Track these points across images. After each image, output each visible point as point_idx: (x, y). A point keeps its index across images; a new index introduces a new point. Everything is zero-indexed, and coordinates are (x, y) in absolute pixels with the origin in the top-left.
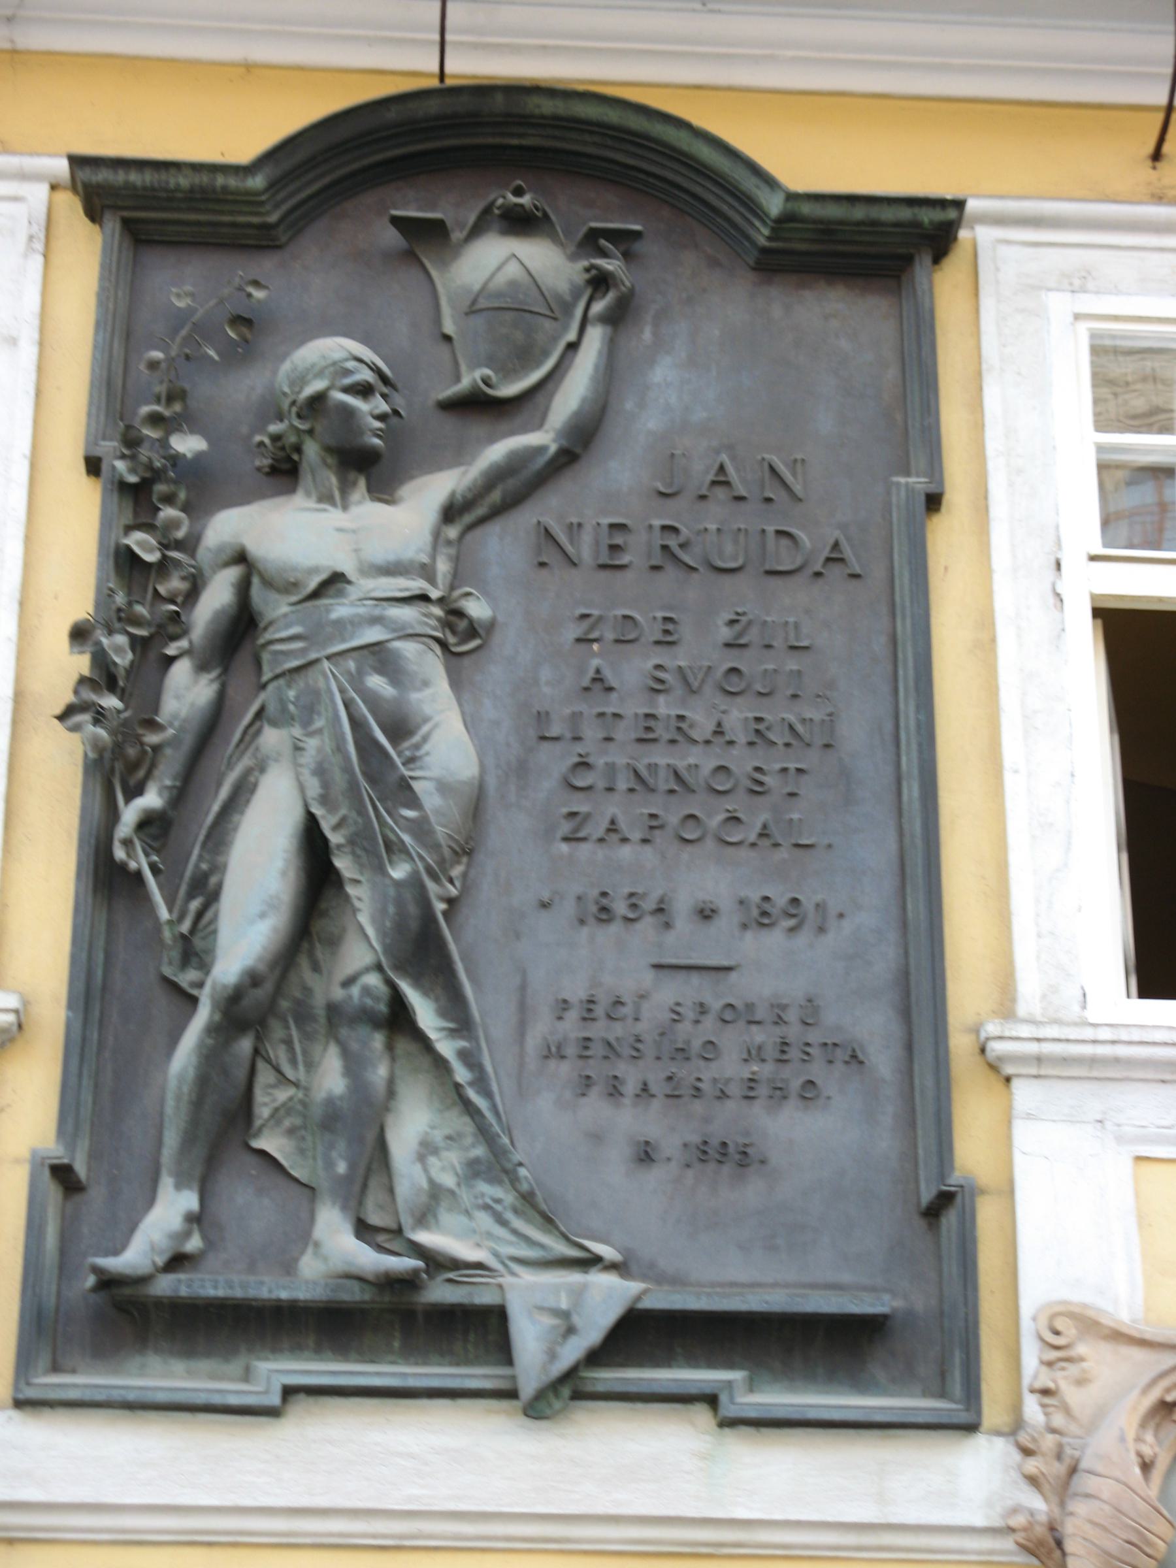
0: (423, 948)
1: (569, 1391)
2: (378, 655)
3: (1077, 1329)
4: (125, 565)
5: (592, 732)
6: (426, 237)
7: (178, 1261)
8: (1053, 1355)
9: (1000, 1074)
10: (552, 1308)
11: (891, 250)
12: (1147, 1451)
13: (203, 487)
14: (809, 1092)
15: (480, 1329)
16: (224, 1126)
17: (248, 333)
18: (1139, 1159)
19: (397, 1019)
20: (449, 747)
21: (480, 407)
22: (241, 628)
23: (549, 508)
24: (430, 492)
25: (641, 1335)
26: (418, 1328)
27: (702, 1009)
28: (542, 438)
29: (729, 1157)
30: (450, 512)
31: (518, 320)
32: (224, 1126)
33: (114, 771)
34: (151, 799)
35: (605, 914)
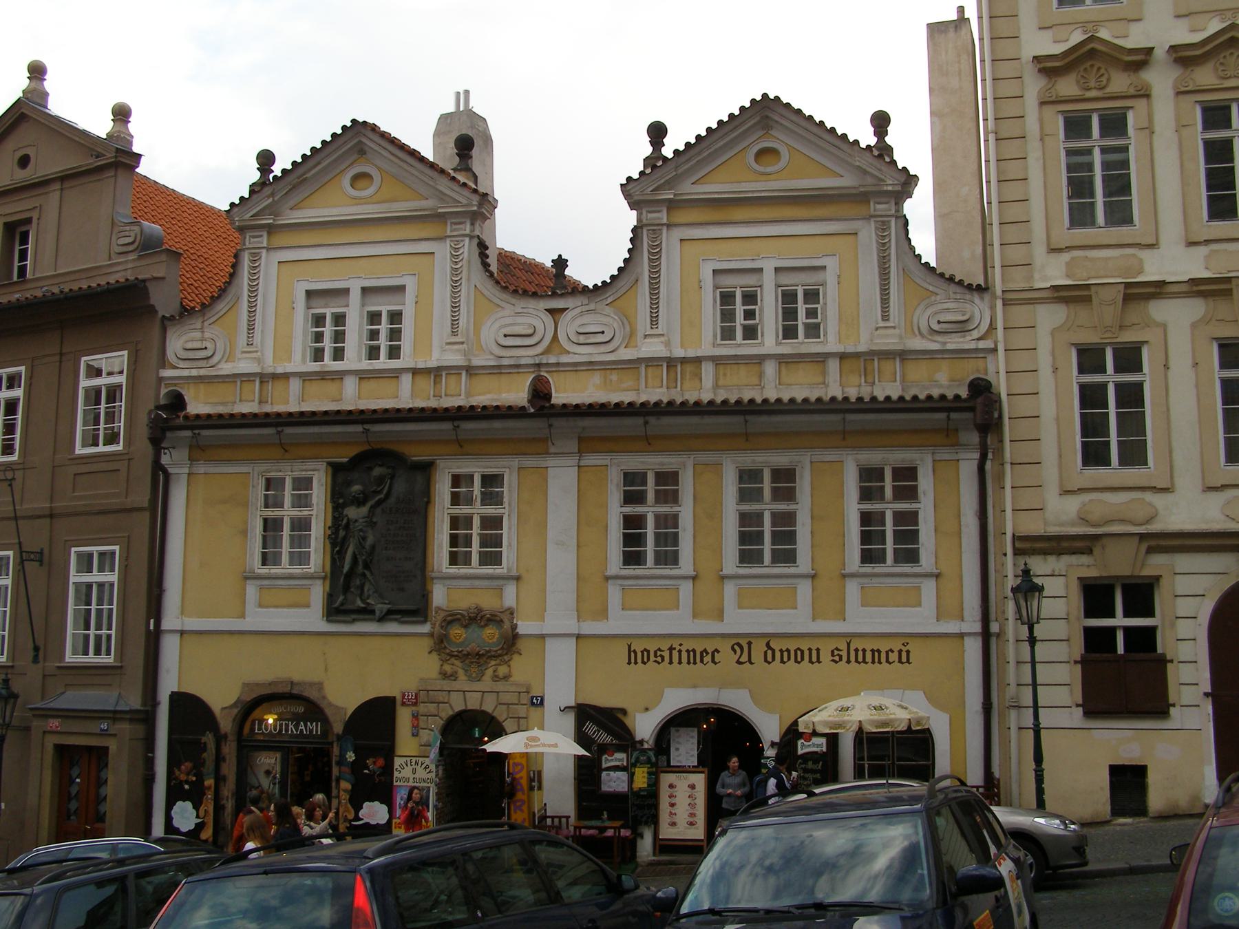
0: (367, 566)
1: (381, 620)
2: (361, 530)
3: (439, 609)
4: (334, 518)
6: (370, 469)
7: (342, 604)
9: (433, 579)
10: (381, 608)
11: (426, 468)
13: (344, 505)
15: (373, 612)
16: (346, 589)
17: (349, 484)
19: (364, 575)
20: (370, 540)
21: (376, 492)
22: (347, 527)
25: (390, 612)
26: (366, 613)
29: (402, 590)
31: (380, 480)
32: (346, 589)
33: (333, 545)
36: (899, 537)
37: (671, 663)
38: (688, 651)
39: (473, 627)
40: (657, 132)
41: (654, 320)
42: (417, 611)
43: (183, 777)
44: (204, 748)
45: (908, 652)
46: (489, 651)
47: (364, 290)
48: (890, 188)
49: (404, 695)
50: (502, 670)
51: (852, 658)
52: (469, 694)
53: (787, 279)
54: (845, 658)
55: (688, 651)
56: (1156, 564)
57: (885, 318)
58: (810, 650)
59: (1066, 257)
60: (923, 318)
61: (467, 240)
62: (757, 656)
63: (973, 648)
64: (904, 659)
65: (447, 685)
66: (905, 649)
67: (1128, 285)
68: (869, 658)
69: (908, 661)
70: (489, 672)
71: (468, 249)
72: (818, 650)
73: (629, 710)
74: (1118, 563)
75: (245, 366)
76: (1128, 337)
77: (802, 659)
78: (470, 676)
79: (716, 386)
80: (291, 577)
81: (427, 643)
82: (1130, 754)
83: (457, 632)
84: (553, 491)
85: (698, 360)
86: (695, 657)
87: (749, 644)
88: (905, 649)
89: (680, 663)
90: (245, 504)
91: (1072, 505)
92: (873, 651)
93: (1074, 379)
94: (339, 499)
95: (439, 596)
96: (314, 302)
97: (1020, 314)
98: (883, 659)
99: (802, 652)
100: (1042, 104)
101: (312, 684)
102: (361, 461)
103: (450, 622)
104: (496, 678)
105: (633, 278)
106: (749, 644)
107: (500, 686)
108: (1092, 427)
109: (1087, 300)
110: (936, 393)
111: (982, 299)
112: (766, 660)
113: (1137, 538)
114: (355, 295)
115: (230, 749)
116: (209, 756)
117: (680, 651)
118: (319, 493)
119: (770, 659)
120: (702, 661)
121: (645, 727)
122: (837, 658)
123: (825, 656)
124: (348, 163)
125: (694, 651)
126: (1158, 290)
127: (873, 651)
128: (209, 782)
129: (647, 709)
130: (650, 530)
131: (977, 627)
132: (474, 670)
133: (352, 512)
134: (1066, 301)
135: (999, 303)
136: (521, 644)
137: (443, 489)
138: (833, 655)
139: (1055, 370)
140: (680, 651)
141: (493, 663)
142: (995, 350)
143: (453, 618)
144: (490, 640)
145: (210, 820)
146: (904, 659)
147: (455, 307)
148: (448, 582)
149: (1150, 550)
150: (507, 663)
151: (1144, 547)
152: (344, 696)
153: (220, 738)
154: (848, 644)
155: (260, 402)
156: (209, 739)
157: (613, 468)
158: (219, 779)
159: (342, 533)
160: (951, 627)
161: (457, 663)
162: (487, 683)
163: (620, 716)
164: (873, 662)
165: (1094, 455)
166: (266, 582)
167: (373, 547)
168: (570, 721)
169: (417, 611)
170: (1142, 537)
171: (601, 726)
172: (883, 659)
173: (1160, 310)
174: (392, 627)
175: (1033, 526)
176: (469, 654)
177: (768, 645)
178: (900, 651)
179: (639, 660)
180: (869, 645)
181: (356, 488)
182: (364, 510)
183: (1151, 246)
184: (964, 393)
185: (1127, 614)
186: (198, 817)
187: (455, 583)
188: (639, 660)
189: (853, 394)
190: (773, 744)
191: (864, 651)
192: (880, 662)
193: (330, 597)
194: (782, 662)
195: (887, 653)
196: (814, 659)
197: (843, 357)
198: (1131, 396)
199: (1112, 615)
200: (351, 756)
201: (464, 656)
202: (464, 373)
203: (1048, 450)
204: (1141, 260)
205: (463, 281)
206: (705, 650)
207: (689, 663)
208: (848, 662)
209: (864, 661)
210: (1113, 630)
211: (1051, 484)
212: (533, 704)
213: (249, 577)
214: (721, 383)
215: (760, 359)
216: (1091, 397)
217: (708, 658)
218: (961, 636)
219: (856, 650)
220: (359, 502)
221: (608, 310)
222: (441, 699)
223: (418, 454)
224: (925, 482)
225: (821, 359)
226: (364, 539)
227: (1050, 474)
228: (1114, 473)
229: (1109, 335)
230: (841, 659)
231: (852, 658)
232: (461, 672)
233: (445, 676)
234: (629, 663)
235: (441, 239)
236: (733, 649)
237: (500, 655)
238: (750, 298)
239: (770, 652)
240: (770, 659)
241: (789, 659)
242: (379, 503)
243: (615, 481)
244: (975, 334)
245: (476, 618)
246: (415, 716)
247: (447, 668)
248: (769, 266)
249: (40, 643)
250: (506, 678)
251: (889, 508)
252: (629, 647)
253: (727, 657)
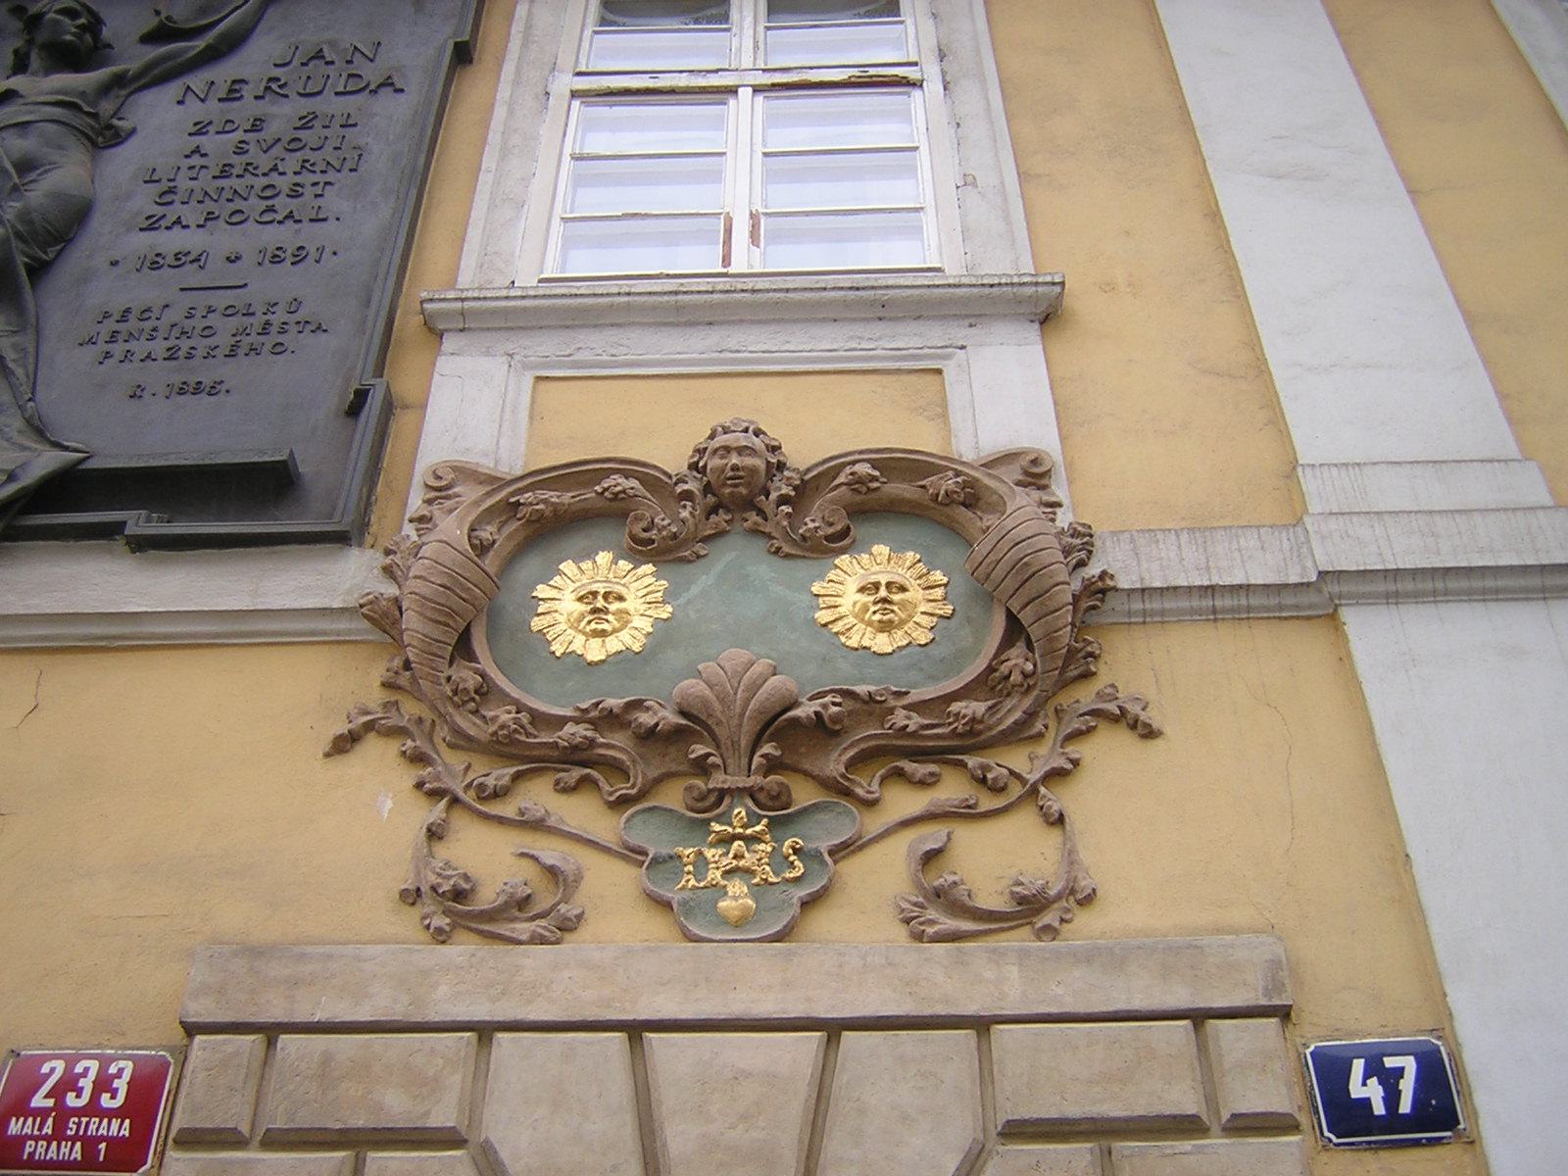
5: (184, 174)
8: (433, 494)
9: (433, 332)
12: (486, 533)
14: (278, 349)
18: (539, 379)
27: (211, 310)
35: (155, 266)
46: (872, 706)
50: (997, 856)
65: (464, 978)
104: (942, 910)
107: (995, 975)
136: (1130, 665)
141: (903, 802)
143: (561, 509)
148: (547, 346)
150: (1039, 797)
161: (583, 813)
176: (694, 723)
212: (1348, 1120)
222: (397, 1107)
232: (609, 884)
233: (454, 908)
237: (973, 738)
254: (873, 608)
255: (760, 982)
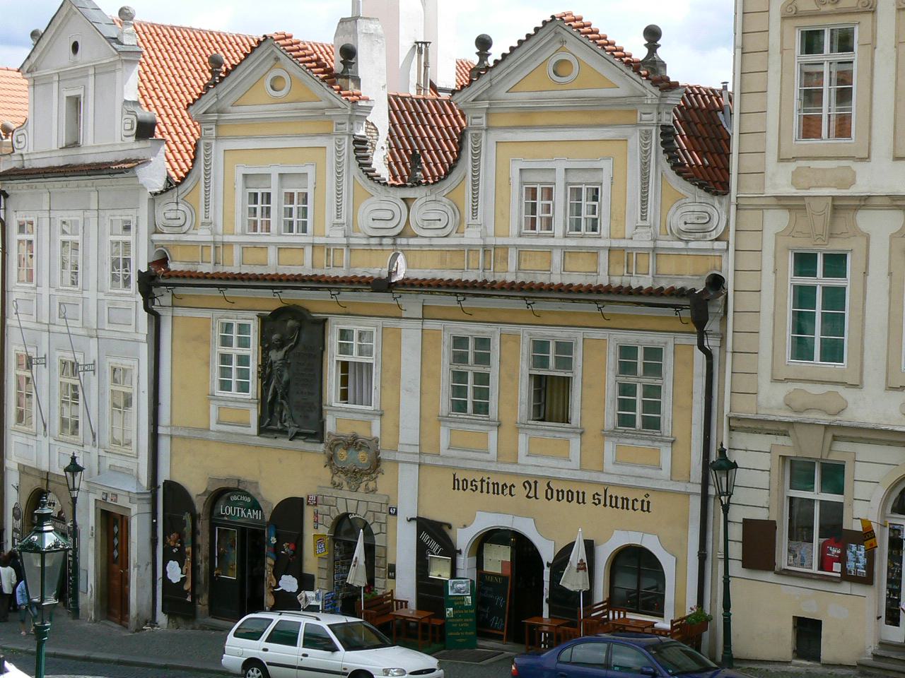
0: (283, 398)
3: (330, 434)
6: (286, 321)
7: (269, 425)
10: (292, 430)
15: (286, 432)
19: (282, 404)
23: (294, 351)
24: (286, 348)
26: (283, 432)
28: (293, 344)
30: (286, 352)
31: (293, 330)
34: (264, 382)
36: (647, 407)
37: (482, 492)
38: (493, 484)
39: (351, 450)
40: (484, 44)
41: (475, 211)
42: (317, 434)
43: (172, 544)
44: (184, 524)
45: (648, 502)
46: (362, 470)
47: (281, 175)
48: (649, 102)
49: (308, 498)
50: (371, 485)
51: (608, 503)
52: (351, 501)
53: (574, 178)
54: (602, 502)
55: (493, 484)
56: (842, 450)
57: (644, 218)
58: (578, 492)
59: (793, 166)
60: (677, 220)
61: (347, 138)
62: (541, 494)
63: (696, 503)
64: (645, 508)
65: (336, 493)
66: (646, 500)
67: (834, 198)
68: (620, 504)
69: (648, 510)
70: (363, 485)
71: (347, 145)
72: (584, 493)
73: (453, 526)
74: (811, 447)
75: (203, 235)
76: (836, 247)
77: (572, 499)
78: (350, 488)
79: (519, 269)
80: (236, 400)
81: (323, 459)
82: (809, 611)
83: (342, 454)
84: (405, 350)
85: (505, 248)
86: (499, 489)
87: (536, 482)
88: (646, 500)
89: (488, 492)
90: (208, 342)
91: (781, 391)
92: (623, 498)
93: (792, 280)
94: (266, 345)
95: (330, 426)
96: (250, 183)
97: (750, 218)
98: (630, 506)
99: (572, 493)
100: (783, 18)
101: (251, 483)
102: (279, 314)
103: (337, 445)
104: (368, 491)
105: (462, 175)
106: (536, 482)
107: (369, 497)
108: (801, 323)
109: (803, 208)
110: (678, 285)
111: (720, 203)
112: (547, 497)
113: (823, 428)
114: (275, 180)
115: (203, 526)
116: (188, 529)
117: (488, 483)
118: (254, 336)
119: (549, 497)
120: (503, 493)
121: (463, 539)
122: (597, 501)
123: (589, 498)
124: (269, 67)
125: (497, 484)
126: (865, 202)
127: (623, 498)
128: (188, 549)
129: (465, 526)
130: (470, 385)
131: (698, 489)
132: (353, 484)
133: (275, 356)
134: (789, 208)
135: (733, 208)
136: (383, 466)
137: (333, 340)
138: (594, 499)
139: (775, 271)
140: (488, 483)
141: (365, 479)
142: (728, 249)
144: (362, 462)
145: (189, 577)
146: (645, 508)
147: (339, 194)
149: (835, 438)
151: (829, 437)
152: (272, 494)
153: (195, 518)
154: (606, 491)
155: (216, 263)
156: (187, 518)
157: (448, 330)
158: (195, 547)
159: (268, 370)
160: (680, 487)
162: (360, 495)
163: (446, 528)
164: (623, 508)
165: (802, 350)
166: (222, 403)
167: (288, 383)
168: (413, 527)
169: (317, 434)
170: (827, 427)
171: (433, 537)
172: (630, 506)
173: (866, 220)
174: (299, 444)
175: (745, 408)
177: (548, 484)
178: (643, 501)
179: (461, 488)
180: (621, 494)
181: (275, 337)
182: (281, 354)
183: (862, 159)
184: (700, 286)
185: (823, 490)
186: (182, 573)
187: (340, 414)
188: (461, 488)
189: (616, 282)
190: (548, 565)
191: (616, 498)
192: (627, 509)
193: (261, 420)
194: (558, 500)
195: (633, 501)
196: (581, 501)
197: (610, 250)
198: (835, 298)
199: (812, 489)
200: (274, 540)
201: (345, 472)
202: (345, 248)
203: (765, 342)
204: (854, 173)
205: (344, 172)
206: (505, 484)
207: (494, 493)
208: (605, 505)
209: (616, 506)
210: (812, 501)
211: (764, 370)
213: (211, 397)
214: (522, 267)
215: (549, 250)
216: (804, 296)
217: (507, 491)
218: (689, 494)
219: (611, 497)
220: (279, 348)
221: (444, 199)
222: (332, 503)
223: (317, 311)
224: (668, 362)
225: (594, 253)
226: (281, 376)
227: (764, 363)
228: (817, 366)
229: (818, 242)
230: (599, 503)
231: (608, 503)
232: (345, 483)
234: (454, 489)
235: (328, 134)
236: (524, 485)
237: (369, 474)
238: (549, 193)
239: (549, 491)
240: (549, 497)
241: (563, 498)
242: (292, 348)
243: (446, 344)
244: (714, 235)
245: (354, 443)
246: (316, 514)
247: (336, 479)
248: (560, 166)
249: (95, 429)
250: (374, 491)
251: (640, 381)
252: (454, 476)
253: (520, 491)
254: (362, 457)
255: (355, 495)
